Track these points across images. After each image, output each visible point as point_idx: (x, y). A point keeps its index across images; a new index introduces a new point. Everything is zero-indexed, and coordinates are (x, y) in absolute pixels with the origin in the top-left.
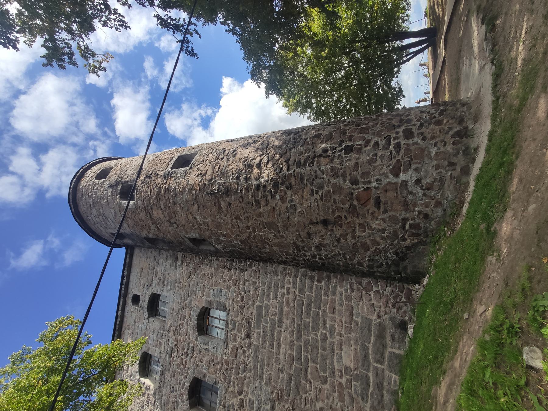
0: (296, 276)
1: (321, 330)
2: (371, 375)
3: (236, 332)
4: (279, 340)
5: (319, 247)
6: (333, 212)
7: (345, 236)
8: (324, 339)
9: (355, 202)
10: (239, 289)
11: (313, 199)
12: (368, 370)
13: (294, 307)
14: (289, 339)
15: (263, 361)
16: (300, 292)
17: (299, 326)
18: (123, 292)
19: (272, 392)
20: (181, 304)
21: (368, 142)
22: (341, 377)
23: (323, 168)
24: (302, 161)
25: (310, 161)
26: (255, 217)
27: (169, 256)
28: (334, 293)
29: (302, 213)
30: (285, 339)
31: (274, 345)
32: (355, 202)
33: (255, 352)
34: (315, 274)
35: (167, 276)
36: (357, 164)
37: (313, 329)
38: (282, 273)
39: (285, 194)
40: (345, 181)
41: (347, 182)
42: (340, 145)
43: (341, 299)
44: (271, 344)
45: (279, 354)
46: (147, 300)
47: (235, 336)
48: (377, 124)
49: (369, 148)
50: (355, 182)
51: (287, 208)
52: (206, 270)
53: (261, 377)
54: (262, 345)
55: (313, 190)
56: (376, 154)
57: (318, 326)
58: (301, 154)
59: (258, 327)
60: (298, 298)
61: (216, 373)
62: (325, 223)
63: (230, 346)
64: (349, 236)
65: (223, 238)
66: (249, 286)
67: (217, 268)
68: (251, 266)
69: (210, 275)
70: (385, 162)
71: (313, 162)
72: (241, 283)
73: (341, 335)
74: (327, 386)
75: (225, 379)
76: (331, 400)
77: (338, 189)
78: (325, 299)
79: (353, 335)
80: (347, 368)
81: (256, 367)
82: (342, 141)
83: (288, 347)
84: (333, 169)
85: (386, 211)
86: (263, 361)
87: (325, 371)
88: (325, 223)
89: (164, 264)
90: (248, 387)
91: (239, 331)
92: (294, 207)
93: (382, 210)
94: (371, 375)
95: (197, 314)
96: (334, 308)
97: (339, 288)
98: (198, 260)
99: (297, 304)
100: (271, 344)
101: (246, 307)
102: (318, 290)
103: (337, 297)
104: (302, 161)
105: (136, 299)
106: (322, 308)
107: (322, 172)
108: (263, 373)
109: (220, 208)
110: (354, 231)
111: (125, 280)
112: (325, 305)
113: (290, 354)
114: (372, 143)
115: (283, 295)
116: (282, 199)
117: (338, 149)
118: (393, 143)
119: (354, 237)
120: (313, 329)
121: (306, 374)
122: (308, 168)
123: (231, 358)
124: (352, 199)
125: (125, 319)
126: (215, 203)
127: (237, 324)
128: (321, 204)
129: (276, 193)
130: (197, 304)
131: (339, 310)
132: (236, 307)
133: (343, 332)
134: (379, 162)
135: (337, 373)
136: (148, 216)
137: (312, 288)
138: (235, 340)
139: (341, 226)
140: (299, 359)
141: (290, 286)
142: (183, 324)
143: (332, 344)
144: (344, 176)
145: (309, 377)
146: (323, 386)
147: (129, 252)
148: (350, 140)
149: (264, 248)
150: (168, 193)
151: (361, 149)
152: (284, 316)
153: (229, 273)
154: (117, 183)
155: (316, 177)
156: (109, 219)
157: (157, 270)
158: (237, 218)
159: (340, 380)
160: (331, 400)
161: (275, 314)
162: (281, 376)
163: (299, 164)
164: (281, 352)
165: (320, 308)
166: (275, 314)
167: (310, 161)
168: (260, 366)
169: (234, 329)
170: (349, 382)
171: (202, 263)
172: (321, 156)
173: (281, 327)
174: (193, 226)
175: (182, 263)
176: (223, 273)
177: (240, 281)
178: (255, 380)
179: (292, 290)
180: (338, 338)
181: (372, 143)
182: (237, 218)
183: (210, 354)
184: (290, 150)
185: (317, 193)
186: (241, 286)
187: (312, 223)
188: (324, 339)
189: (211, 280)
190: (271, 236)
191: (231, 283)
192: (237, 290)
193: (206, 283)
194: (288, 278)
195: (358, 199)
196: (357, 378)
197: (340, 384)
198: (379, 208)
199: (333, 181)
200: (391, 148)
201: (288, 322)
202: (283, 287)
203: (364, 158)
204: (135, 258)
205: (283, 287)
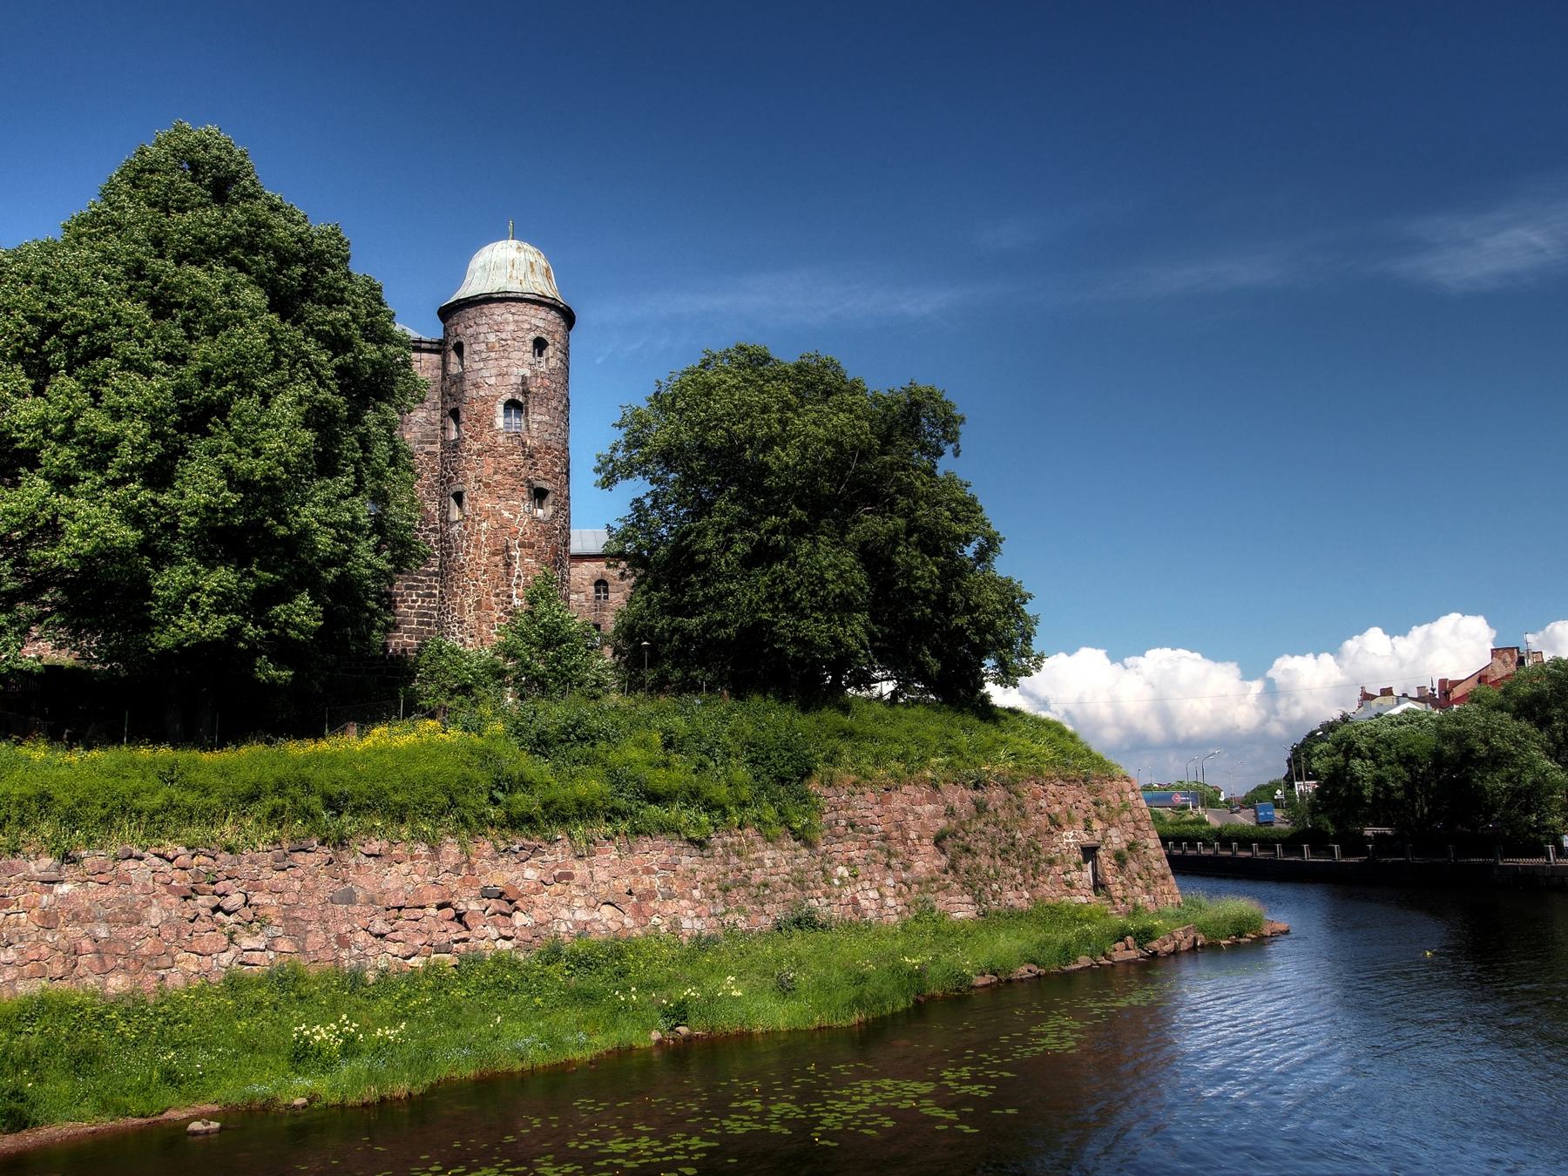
27: (433, 428)
65: (465, 544)
98: (432, 480)
109: (494, 554)
116: (499, 618)
129: (505, 613)
136: (487, 448)
147: (435, 347)
149: (458, 588)
154: (525, 393)
156: (482, 365)
158: (485, 572)
182: (485, 572)
190: (470, 601)
205: (418, 595)
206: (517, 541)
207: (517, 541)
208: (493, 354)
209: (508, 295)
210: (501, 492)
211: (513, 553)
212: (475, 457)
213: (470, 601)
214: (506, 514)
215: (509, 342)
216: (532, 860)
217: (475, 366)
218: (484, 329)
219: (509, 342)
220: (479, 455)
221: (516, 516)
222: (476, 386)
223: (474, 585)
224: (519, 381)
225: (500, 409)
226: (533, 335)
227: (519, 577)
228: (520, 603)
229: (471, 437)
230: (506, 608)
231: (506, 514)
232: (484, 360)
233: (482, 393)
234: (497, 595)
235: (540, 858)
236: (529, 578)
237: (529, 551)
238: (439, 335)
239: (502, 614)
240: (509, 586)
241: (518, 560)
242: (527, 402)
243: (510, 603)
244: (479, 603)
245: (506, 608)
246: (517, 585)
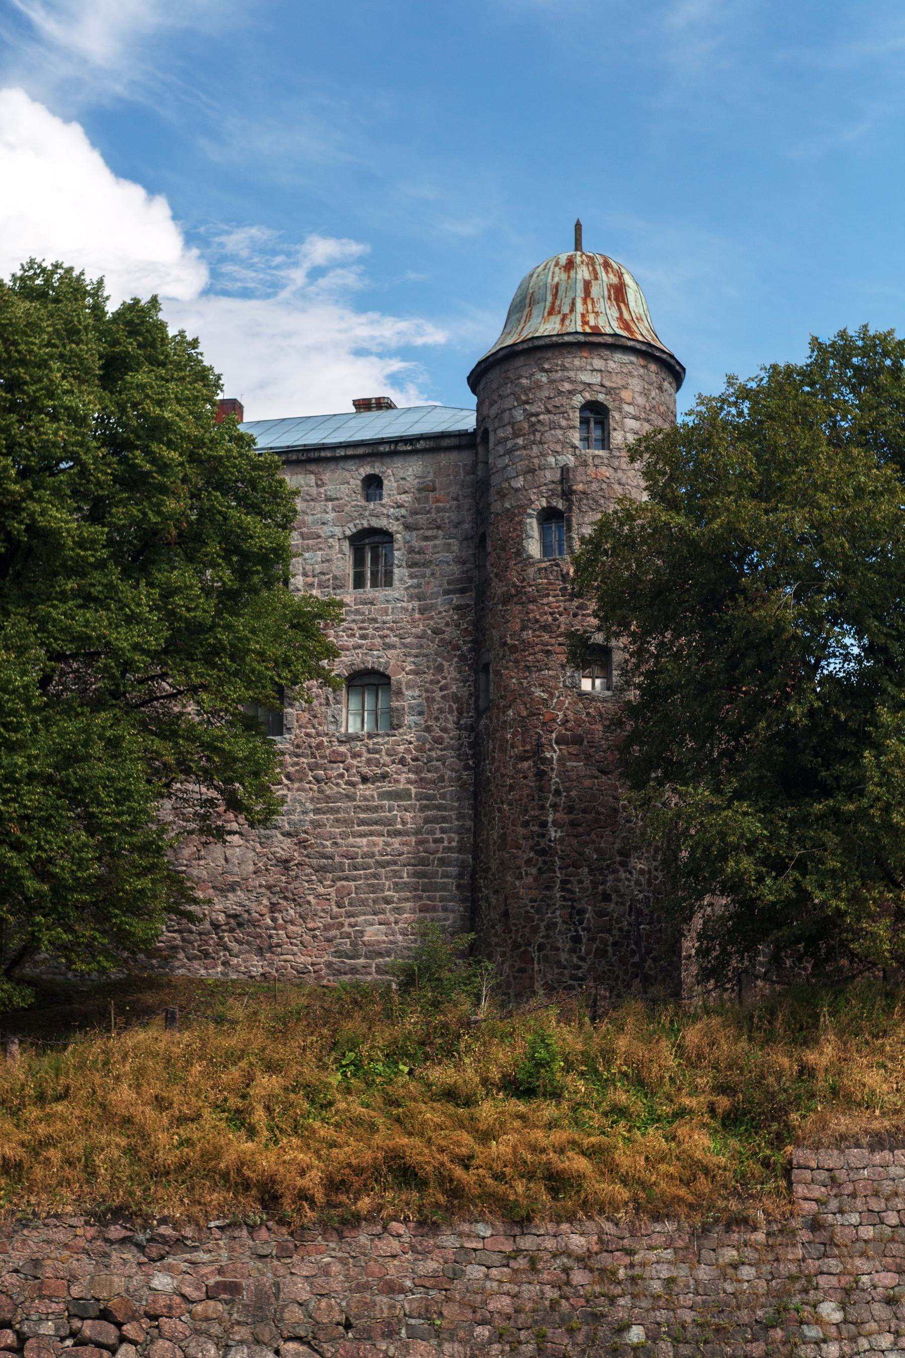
0: (460, 850)
1: (397, 895)
2: (362, 961)
3: (366, 755)
4: (371, 835)
5: (487, 899)
6: (515, 925)
7: (496, 935)
8: (387, 901)
9: (523, 949)
10: (430, 750)
11: (527, 902)
12: (366, 958)
13: (419, 852)
14: (376, 850)
15: (337, 810)
16: (440, 859)
17: (395, 863)
18: (381, 448)
19: (306, 832)
20: (384, 623)
21: (582, 959)
22: (350, 925)
23: (558, 913)
24: (569, 886)
25: (567, 895)
26: (512, 817)
28: (445, 909)
29: (515, 887)
30: (375, 844)
31: (362, 828)
32: (523, 949)
33: (347, 796)
34: (466, 880)
35: (428, 571)
36: (558, 949)
37: (396, 884)
38: (462, 827)
39: (535, 866)
40: (543, 937)
41: (541, 940)
42: (584, 929)
43: (439, 920)
44: (362, 823)
45: (354, 837)
46: (376, 523)
47: (360, 756)
48: (612, 965)
49: (575, 960)
50: (541, 947)
51: (519, 868)
52: (451, 671)
53: (316, 811)
54: (359, 807)
55: (535, 901)
56: (565, 968)
57: (402, 890)
58: (580, 882)
59: (382, 796)
60: (431, 857)
61: (300, 727)
62: (506, 914)
63: (342, 749)
64: (496, 940)
66: (437, 769)
67: (456, 698)
68: (467, 768)
69: (443, 682)
70: (556, 977)
71: (564, 899)
72: (439, 753)
73: (396, 923)
74: (335, 909)
75: (298, 746)
76: (322, 914)
77: (535, 930)
78: (435, 897)
79: (400, 938)
80: (362, 932)
81: (328, 799)
82: (588, 929)
83: (365, 849)
84: (556, 924)
85: (515, 978)
86: (337, 810)
87: (351, 904)
88: (506, 914)
89: (451, 556)
90: (298, 790)
91: (369, 762)
92: (519, 877)
93: (517, 974)
94: (362, 961)
95: (376, 666)
96: (427, 911)
97: (451, 916)
99: (423, 858)
100: (362, 823)
101: (405, 769)
102: (444, 887)
103: (441, 914)
104: (569, 886)
105: (373, 484)
106: (425, 894)
107: (554, 912)
108: (324, 813)
109: (523, 759)
110: (500, 946)
111: (405, 448)
112: (429, 898)
113: (357, 853)
114: (580, 963)
115: (432, 832)
116: (528, 862)
117: (579, 928)
118: (575, 983)
119: (497, 945)
120: (396, 884)
121: (341, 879)
122: (558, 895)
123: (328, 752)
124: (526, 945)
125: (332, 466)
126: (525, 751)
127: (377, 756)
128: (522, 911)
130: (392, 662)
131: (425, 918)
132: (401, 749)
133: (400, 925)
134: (556, 971)
135: (352, 920)
137: (447, 877)
138: (355, 755)
139: (504, 932)
140: (356, 869)
141: (446, 844)
142: (353, 635)
143: (383, 912)
144: (547, 937)
145: (339, 884)
146: (333, 903)
148: (589, 940)
150: (542, 651)
151: (575, 952)
152: (405, 839)
153: (450, 726)
154: (567, 494)
155: (548, 905)
157: (435, 537)
159: (346, 924)
160: (322, 914)
161: (404, 823)
162: (328, 843)
163: (564, 882)
164: (358, 840)
165: (423, 891)
166: (404, 823)
167: (567, 895)
168: (332, 808)
169: (369, 751)
170: (348, 936)
171: (462, 658)
172: (573, 907)
173: (389, 835)
174: (502, 697)
175: (457, 608)
176: (451, 711)
177: (441, 750)
178: (312, 800)
179: (441, 846)
180: (392, 919)
181: (580, 963)
183: (323, 709)
184: (589, 866)
185: (532, 907)
186: (433, 754)
187: (506, 898)
188: (387, 901)
189: (435, 687)
191: (438, 733)
192: (427, 746)
193: (429, 677)
194: (456, 839)
195: (526, 951)
196: (354, 944)
197: (342, 925)
198: (518, 971)
199: (542, 925)
200: (571, 982)
201: (397, 846)
202: (443, 831)
203: (563, 956)
204: (454, 456)
206: (554, 735)
207: (554, 735)
208: (520, 441)
209: (536, 343)
210: (530, 658)
211: (548, 755)
212: (500, 607)
213: (495, 835)
214: (538, 693)
215: (541, 417)
216: (169, 1260)
217: (500, 463)
218: (510, 402)
219: (541, 417)
220: (504, 604)
221: (552, 695)
222: (502, 495)
223: (499, 810)
224: (558, 476)
225: (533, 526)
226: (578, 400)
227: (557, 792)
228: (559, 834)
229: (497, 575)
230: (538, 844)
231: (538, 693)
232: (510, 452)
233: (507, 505)
234: (526, 824)
235: (188, 1256)
236: (573, 793)
237: (574, 749)
238: (469, 422)
239: (532, 854)
240: (542, 808)
241: (555, 766)
242: (570, 509)
243: (543, 836)
244: (503, 837)
245: (538, 844)
246: (554, 806)
